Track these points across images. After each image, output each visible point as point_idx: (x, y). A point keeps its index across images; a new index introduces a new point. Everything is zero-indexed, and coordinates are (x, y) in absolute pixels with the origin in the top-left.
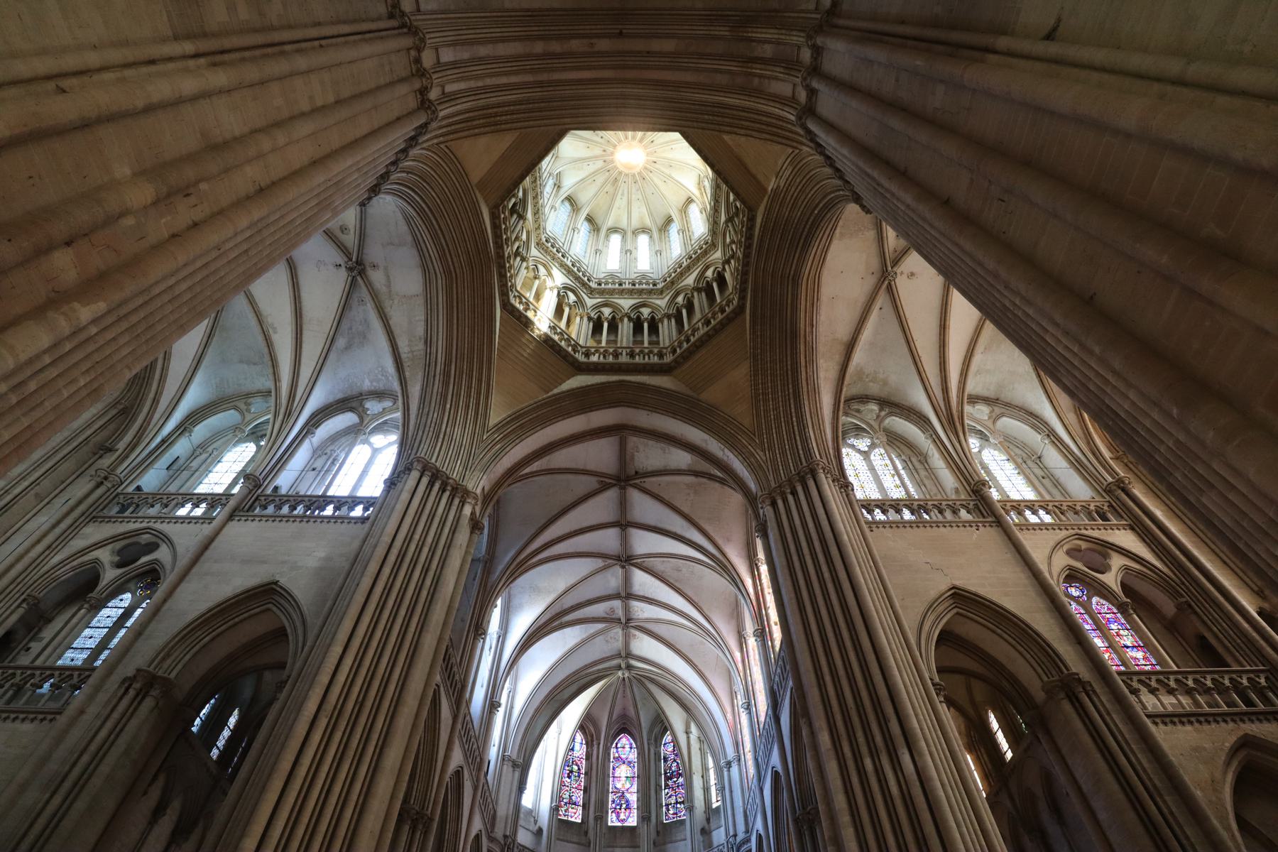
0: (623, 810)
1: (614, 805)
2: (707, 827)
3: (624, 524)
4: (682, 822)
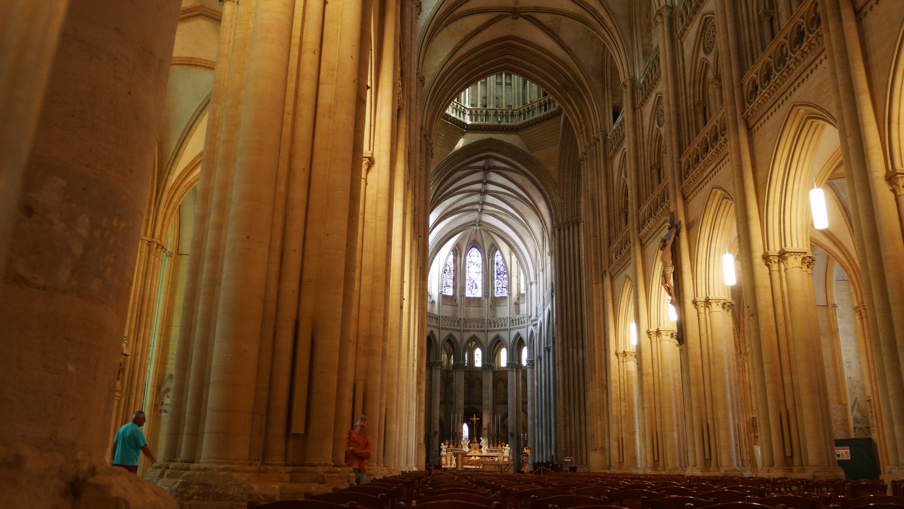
0: (474, 289)
1: (469, 286)
2: (517, 302)
3: (485, 182)
4: (505, 297)
